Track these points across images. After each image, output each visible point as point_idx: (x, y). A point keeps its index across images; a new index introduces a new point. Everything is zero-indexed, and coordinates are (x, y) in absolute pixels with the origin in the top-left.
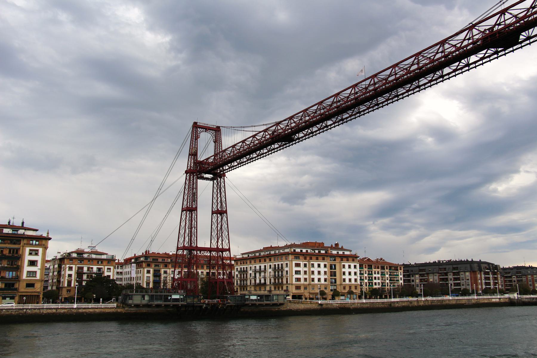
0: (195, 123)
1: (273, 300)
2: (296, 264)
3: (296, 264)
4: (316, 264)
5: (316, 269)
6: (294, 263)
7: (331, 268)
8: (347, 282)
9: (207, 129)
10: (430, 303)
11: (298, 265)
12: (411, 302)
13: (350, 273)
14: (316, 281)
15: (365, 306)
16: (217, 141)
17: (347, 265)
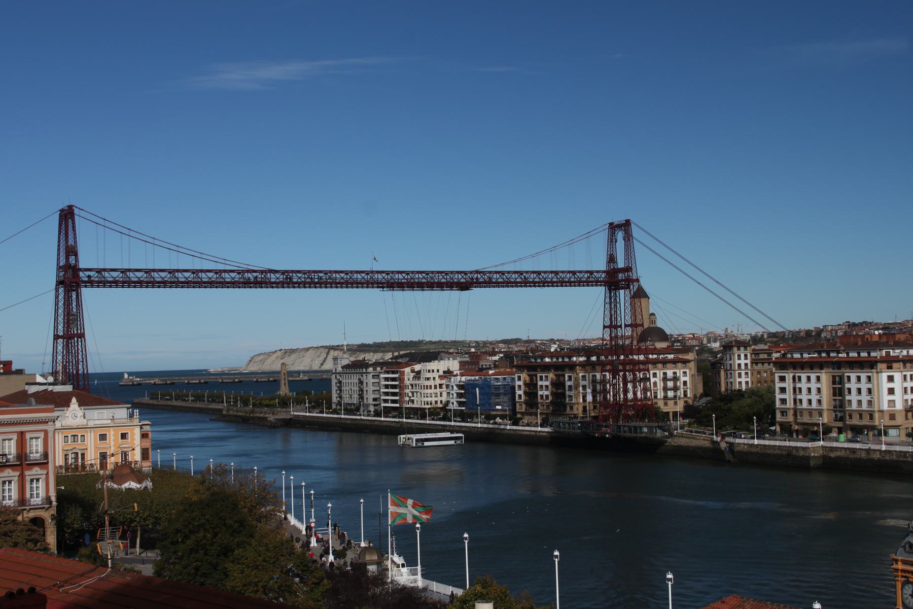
0: (611, 224)
1: (641, 432)
2: (780, 377)
3: (780, 377)
4: (804, 377)
5: (803, 385)
6: (777, 375)
7: (834, 383)
8: (854, 406)
9: (619, 226)
10: (895, 457)
11: (782, 379)
12: (853, 451)
13: (859, 391)
14: (805, 405)
15: (754, 450)
16: (628, 238)
17: (853, 376)
